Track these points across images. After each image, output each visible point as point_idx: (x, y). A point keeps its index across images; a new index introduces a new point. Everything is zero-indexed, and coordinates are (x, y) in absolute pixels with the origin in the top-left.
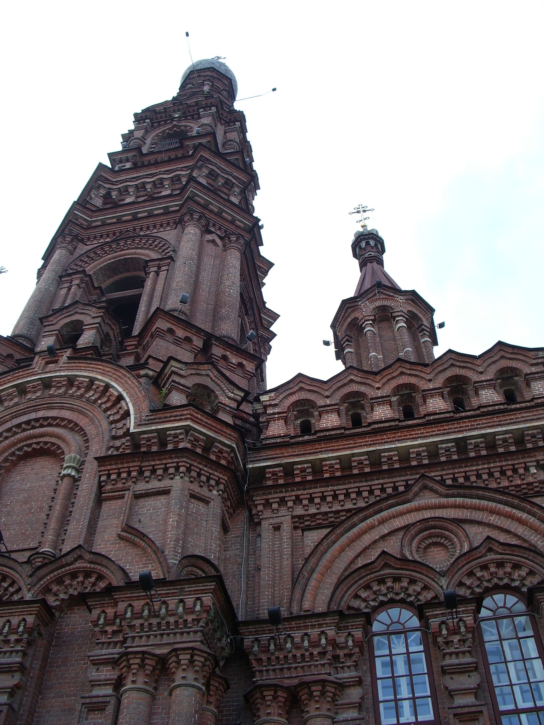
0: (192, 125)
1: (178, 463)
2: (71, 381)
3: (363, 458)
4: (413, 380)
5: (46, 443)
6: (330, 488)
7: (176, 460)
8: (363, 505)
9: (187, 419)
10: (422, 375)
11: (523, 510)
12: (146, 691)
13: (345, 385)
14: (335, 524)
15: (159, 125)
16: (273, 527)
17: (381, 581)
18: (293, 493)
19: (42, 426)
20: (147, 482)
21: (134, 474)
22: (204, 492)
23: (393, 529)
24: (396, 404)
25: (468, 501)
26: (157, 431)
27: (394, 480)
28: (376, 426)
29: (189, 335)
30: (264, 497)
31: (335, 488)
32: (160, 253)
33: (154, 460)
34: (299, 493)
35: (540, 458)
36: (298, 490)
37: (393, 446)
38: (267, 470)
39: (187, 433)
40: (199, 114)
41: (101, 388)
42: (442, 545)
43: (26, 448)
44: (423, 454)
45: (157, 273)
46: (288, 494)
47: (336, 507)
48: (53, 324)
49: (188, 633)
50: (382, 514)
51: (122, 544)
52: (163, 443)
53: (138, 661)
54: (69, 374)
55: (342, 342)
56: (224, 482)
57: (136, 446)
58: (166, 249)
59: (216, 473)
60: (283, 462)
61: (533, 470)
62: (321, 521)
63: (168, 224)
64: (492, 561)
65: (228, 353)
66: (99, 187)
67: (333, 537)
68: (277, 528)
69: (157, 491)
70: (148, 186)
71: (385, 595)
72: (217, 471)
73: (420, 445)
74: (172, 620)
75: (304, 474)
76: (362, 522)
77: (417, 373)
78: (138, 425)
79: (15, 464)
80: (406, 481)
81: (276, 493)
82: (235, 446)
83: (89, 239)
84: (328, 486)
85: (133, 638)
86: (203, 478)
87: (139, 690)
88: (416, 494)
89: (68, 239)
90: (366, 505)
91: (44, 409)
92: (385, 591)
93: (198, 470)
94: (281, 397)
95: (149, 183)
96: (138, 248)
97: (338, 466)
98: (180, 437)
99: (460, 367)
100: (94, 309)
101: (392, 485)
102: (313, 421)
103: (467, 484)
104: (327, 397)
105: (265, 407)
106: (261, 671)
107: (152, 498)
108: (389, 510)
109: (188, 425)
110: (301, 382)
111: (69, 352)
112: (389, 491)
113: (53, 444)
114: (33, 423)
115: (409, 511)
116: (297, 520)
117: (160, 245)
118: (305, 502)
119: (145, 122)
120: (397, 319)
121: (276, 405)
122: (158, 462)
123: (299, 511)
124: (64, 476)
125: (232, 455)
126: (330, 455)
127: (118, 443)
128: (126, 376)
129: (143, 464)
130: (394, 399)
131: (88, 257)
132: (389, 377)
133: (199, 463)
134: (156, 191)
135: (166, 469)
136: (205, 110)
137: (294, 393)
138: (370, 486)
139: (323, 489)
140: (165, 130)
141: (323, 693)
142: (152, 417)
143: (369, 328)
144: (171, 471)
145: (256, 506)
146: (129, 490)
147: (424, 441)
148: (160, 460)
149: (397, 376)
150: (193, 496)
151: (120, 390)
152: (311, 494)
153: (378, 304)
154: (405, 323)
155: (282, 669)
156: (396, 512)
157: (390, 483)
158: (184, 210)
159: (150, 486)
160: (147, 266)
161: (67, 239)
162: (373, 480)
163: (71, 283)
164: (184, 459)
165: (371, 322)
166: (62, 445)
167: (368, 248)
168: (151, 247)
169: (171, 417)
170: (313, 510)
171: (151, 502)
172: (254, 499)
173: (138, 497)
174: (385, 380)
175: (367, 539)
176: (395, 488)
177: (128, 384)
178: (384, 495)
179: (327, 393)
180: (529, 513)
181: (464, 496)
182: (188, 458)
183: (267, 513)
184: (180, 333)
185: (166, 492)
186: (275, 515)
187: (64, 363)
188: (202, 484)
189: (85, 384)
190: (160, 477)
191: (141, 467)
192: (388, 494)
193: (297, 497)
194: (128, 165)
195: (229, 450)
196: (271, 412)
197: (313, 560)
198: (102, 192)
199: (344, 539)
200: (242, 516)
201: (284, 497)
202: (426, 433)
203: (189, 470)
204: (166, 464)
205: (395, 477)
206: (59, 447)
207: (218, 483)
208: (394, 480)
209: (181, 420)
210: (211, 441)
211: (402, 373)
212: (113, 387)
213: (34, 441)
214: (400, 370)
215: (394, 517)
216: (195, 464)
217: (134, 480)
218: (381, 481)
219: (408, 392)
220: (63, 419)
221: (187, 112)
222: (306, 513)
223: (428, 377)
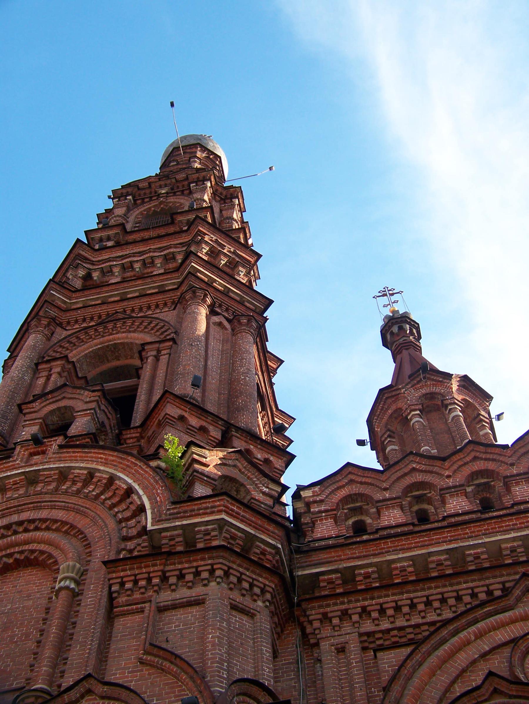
0: (182, 201)
1: (212, 565)
3: (442, 557)
4: (491, 466)
5: (32, 551)
7: (210, 562)
8: (451, 615)
9: (220, 511)
13: (406, 474)
14: (415, 642)
15: (143, 202)
16: (336, 649)
18: (358, 604)
19: (26, 530)
20: (173, 590)
21: (156, 581)
22: (247, 601)
23: (495, 645)
24: (471, 495)
26: (182, 527)
27: (487, 582)
28: (453, 520)
29: (205, 424)
30: (321, 610)
31: (412, 595)
32: (158, 336)
33: (180, 563)
34: (366, 603)
36: (365, 599)
37: (480, 541)
38: (321, 578)
39: (221, 529)
40: (190, 188)
41: (105, 481)
43: (5, 559)
44: (518, 550)
45: (157, 358)
46: (351, 606)
47: (416, 620)
48: (35, 412)
50: (479, 625)
51: (146, 671)
54: (62, 465)
55: (383, 439)
56: (270, 590)
58: (166, 331)
59: (260, 579)
60: (341, 566)
62: (397, 639)
63: (165, 304)
65: (252, 447)
66: (77, 267)
67: (418, 657)
68: (341, 650)
69: (187, 602)
70: (137, 266)
72: (261, 576)
73: (514, 539)
75: (368, 581)
76: (454, 636)
77: (495, 457)
78: (155, 521)
80: (503, 583)
81: (335, 604)
82: (280, 546)
83: (68, 323)
84: (402, 593)
86: (246, 585)
88: (519, 600)
89: (44, 322)
90: (454, 615)
91: (29, 509)
93: (239, 575)
94: (328, 491)
95: (137, 261)
96: (130, 332)
97: (411, 569)
98: (213, 533)
100: (86, 393)
101: (485, 589)
104: (386, 489)
105: (308, 505)
107: (181, 611)
108: (487, 621)
109: (223, 519)
110: (350, 473)
111: (60, 440)
112: (483, 596)
113: (42, 552)
114: (14, 527)
115: (513, 621)
116: (365, 638)
117: (158, 327)
118: (375, 615)
119: (126, 199)
120: (450, 407)
121: (322, 501)
122: (187, 565)
123: (368, 626)
124: (61, 589)
125: (278, 557)
126: (400, 556)
127: (130, 545)
128: (136, 465)
129: (168, 568)
130: (469, 489)
131: (69, 342)
133: (239, 565)
134: (146, 271)
135: (197, 574)
136: (197, 185)
137: (343, 486)
138: (457, 591)
139: (396, 598)
140: (150, 208)
142: (175, 511)
143: (417, 419)
144: (205, 575)
145: (311, 622)
146: (150, 601)
147: (519, 534)
148: (189, 562)
149: (471, 461)
150: (234, 607)
151: (130, 481)
152: (381, 605)
153: (424, 391)
156: (497, 622)
157: (483, 586)
158: (184, 288)
159: (177, 595)
160: (143, 349)
161: (43, 322)
162: (459, 583)
163: (50, 371)
164: (221, 561)
165: (418, 412)
166: (56, 553)
167: (400, 334)
168: (146, 330)
169: (199, 509)
170: (385, 625)
171: (179, 615)
172: (308, 613)
173: (161, 610)
174: (455, 467)
176: (489, 593)
177: (139, 474)
179: (385, 485)
182: (223, 557)
183: (327, 631)
184: (194, 421)
185: (199, 602)
186: (336, 633)
187: (54, 453)
188: (244, 592)
189: (83, 477)
190: (190, 584)
192: (481, 601)
193: (364, 608)
194: (110, 244)
195: (273, 551)
196: (317, 510)
197: (396, 687)
198: (81, 273)
199: (433, 660)
200: (293, 636)
201: (346, 610)
202: (520, 524)
203: (227, 574)
204: (197, 567)
205: (488, 578)
206: (50, 556)
207: (263, 591)
209: (212, 513)
210: (250, 539)
211: (475, 458)
212: (120, 478)
213: (17, 549)
214: (473, 454)
215: (494, 629)
216: (235, 567)
217: (156, 588)
218: (471, 585)
219: (486, 480)
220: (56, 521)
221: (175, 188)
222: (377, 628)
223: (510, 460)
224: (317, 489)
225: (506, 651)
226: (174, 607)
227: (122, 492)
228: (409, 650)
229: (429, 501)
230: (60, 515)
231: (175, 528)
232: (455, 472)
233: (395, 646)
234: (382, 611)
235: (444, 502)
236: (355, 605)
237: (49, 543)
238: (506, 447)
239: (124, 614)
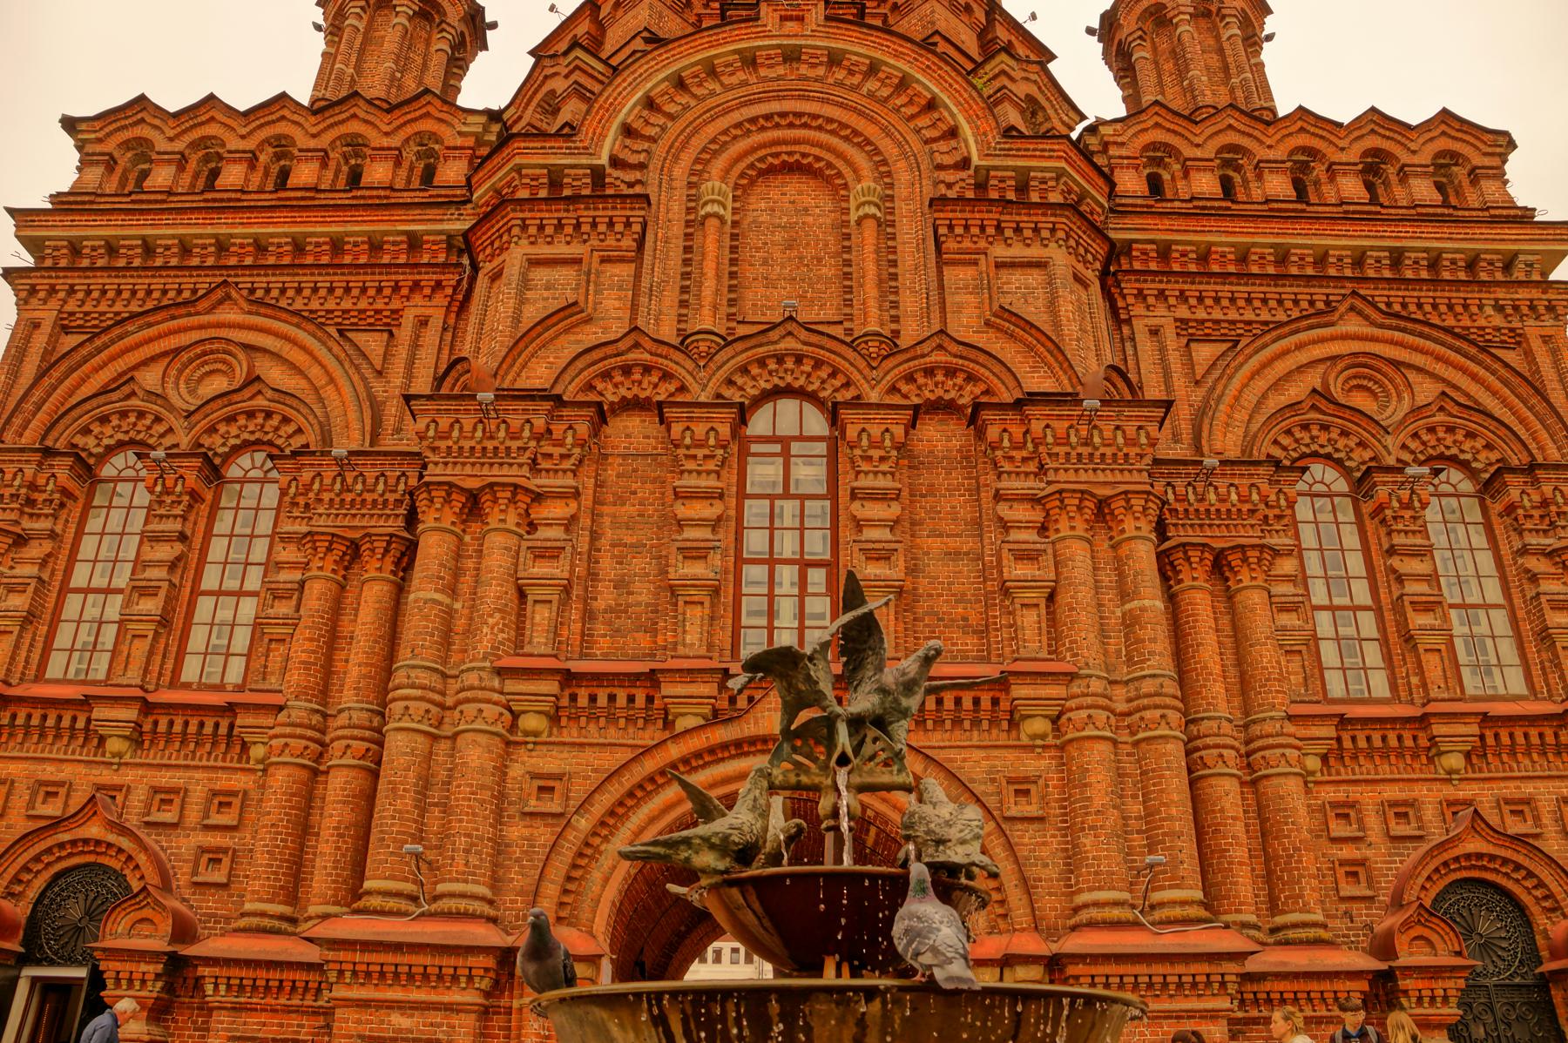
2: (835, 59)
5: (804, 155)
6: (1227, 288)
10: (1332, 138)
11: (1479, 363)
12: (1088, 541)
17: (1305, 427)
25: (1409, 338)
26: (1014, 169)
27: (1312, 290)
34: (1186, 287)
35: (1501, 296)
39: (1057, 179)
42: (1368, 389)
46: (1169, 286)
49: (1130, 471)
52: (1023, 188)
53: (1076, 502)
57: (981, 186)
61: (1489, 311)
64: (1442, 424)
71: (1307, 445)
73: (1343, 248)
74: (1109, 451)
77: (1324, 133)
79: (752, 182)
85: (1057, 470)
87: (1081, 538)
88: (1341, 318)
92: (1307, 441)
99: (1384, 136)
102: (1166, 176)
103: (1404, 313)
106: (1175, 525)
113: (818, 159)
114: (777, 119)
121: (1123, 144)
123: (1183, 312)
132: (1285, 132)
141: (1260, 560)
144: (1046, 234)
145: (1124, 297)
151: (936, 90)
155: (1201, 526)
166: (840, 164)
173: (999, 266)
175: (1281, 367)
178: (1312, 311)
180: (1487, 368)
181: (1404, 330)
185: (1040, 265)
191: (999, 222)
193: (1182, 292)
199: (1254, 362)
206: (830, 165)
208: (1312, 290)
214: (1300, 124)
215: (1314, 342)
218: (1295, 290)
224: (1118, 126)
225: (1321, 369)
226: (1012, 265)
227: (923, 102)
228: (1225, 346)
229: (1238, 169)
230: (836, 113)
231: (1006, 168)
232: (1278, 141)
233: (1207, 340)
234: (1200, 299)
235: (1260, 177)
236: (1172, 288)
237: (830, 149)
238: (1340, 125)
239: (954, 263)
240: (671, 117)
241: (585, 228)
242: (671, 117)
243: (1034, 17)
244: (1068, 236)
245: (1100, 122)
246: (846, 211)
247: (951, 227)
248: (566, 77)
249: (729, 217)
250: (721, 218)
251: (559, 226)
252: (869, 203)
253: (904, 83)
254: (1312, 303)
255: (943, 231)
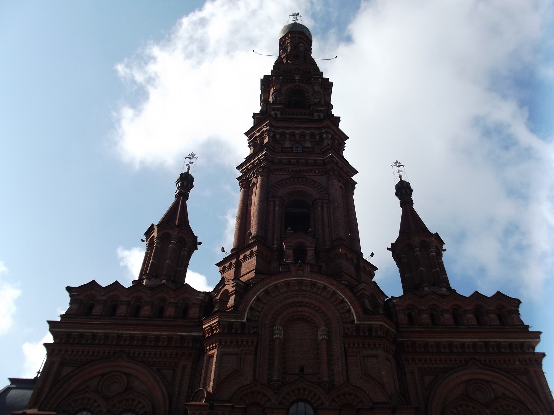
2: (313, 284)
9: (380, 321)
26: (368, 324)
45: (322, 208)
61: (517, 363)
70: (297, 137)
102: (413, 314)
144: (377, 346)
154: (435, 252)
167: (404, 191)
185: (376, 356)
238: (467, 297)
240: (265, 304)
241: (240, 343)
242: (265, 304)
243: (372, 255)
244: (384, 346)
245: (393, 298)
246: (317, 335)
247: (349, 344)
248: (233, 287)
249: (281, 337)
250: (279, 338)
251: (231, 342)
252: (324, 334)
253: (334, 293)
254: (460, 361)
255: (346, 345)
